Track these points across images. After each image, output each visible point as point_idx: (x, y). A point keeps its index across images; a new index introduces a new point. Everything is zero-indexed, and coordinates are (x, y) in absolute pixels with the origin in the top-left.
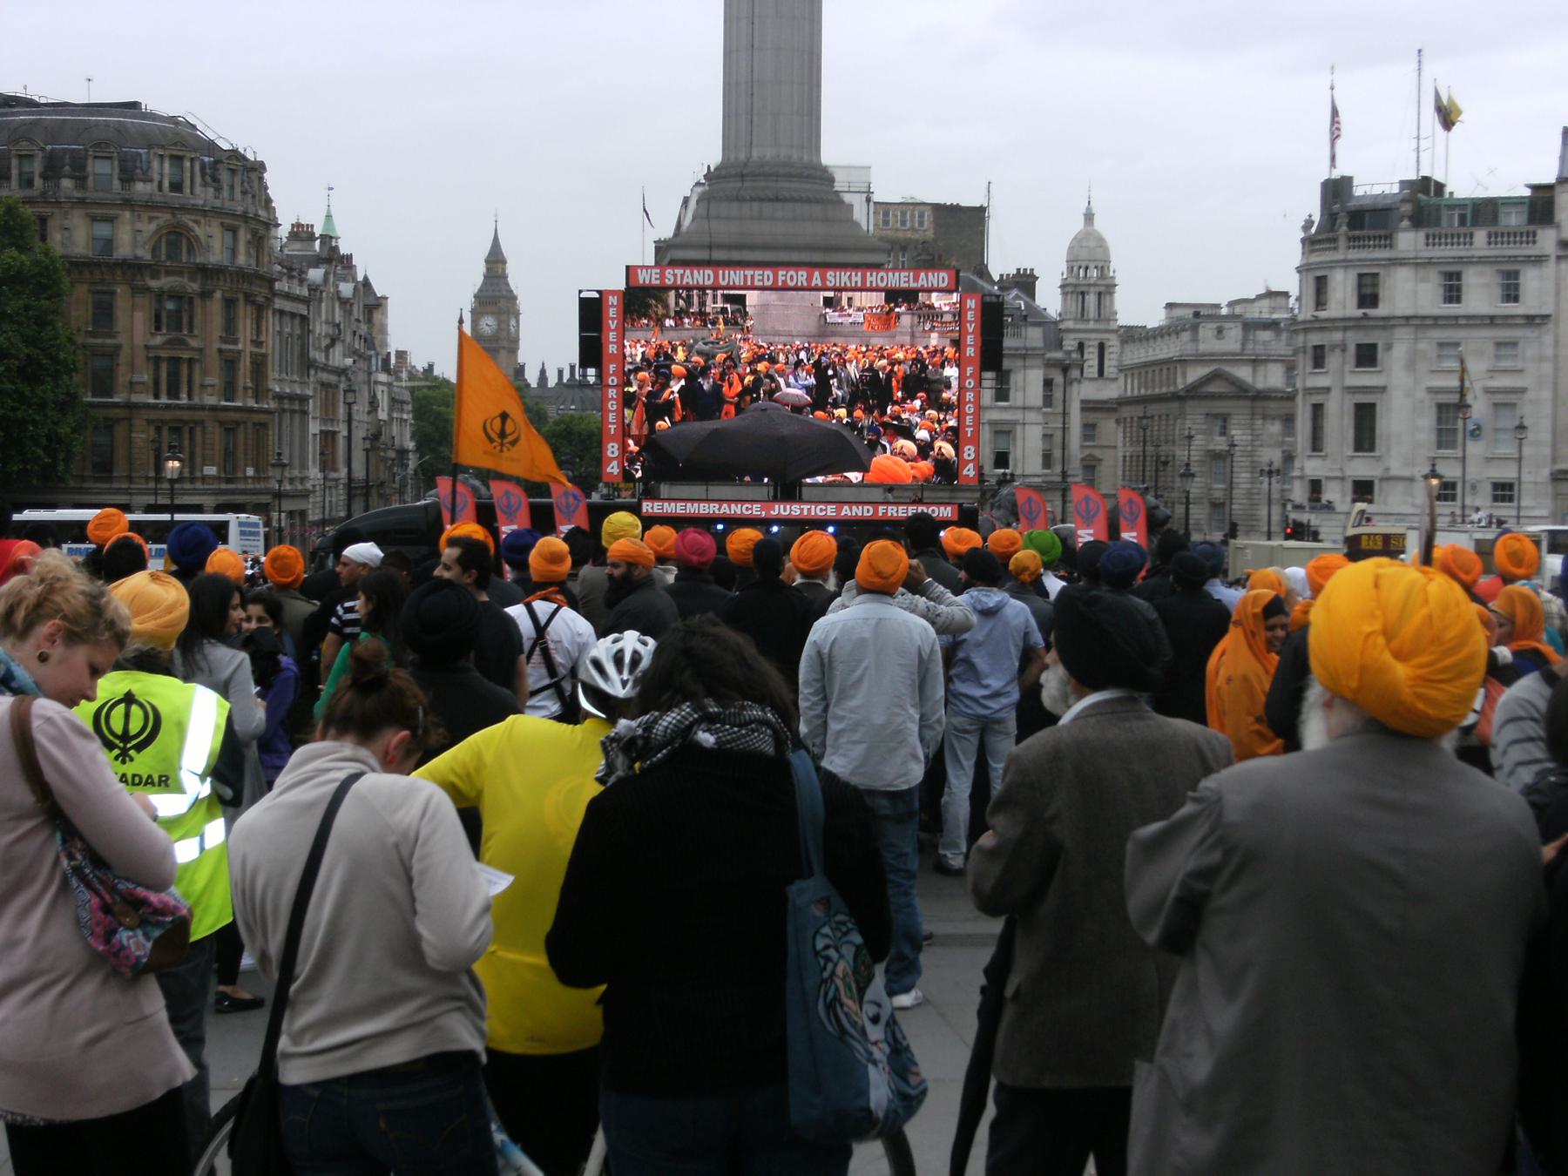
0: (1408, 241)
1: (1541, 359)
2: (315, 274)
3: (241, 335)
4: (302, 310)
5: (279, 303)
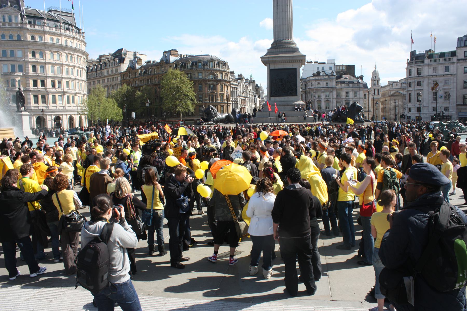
0: (427, 61)
1: (454, 83)
2: (239, 81)
3: (224, 91)
4: (237, 87)
5: (231, 86)
